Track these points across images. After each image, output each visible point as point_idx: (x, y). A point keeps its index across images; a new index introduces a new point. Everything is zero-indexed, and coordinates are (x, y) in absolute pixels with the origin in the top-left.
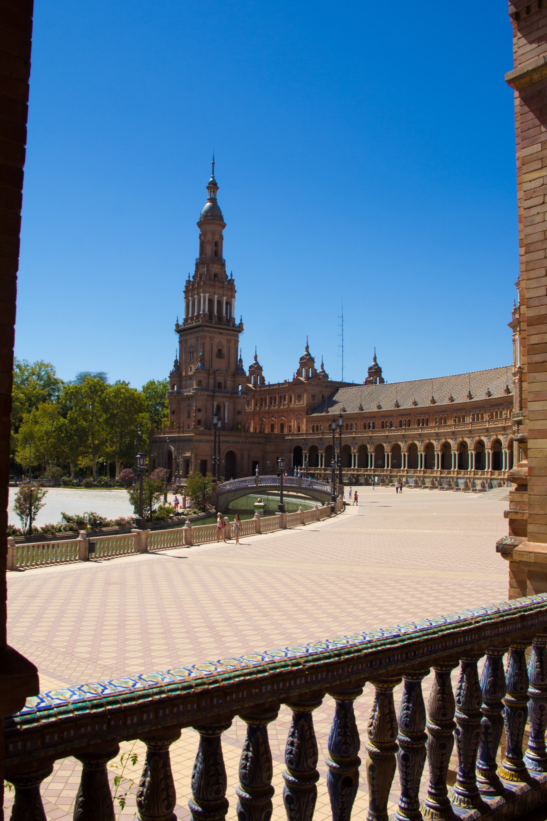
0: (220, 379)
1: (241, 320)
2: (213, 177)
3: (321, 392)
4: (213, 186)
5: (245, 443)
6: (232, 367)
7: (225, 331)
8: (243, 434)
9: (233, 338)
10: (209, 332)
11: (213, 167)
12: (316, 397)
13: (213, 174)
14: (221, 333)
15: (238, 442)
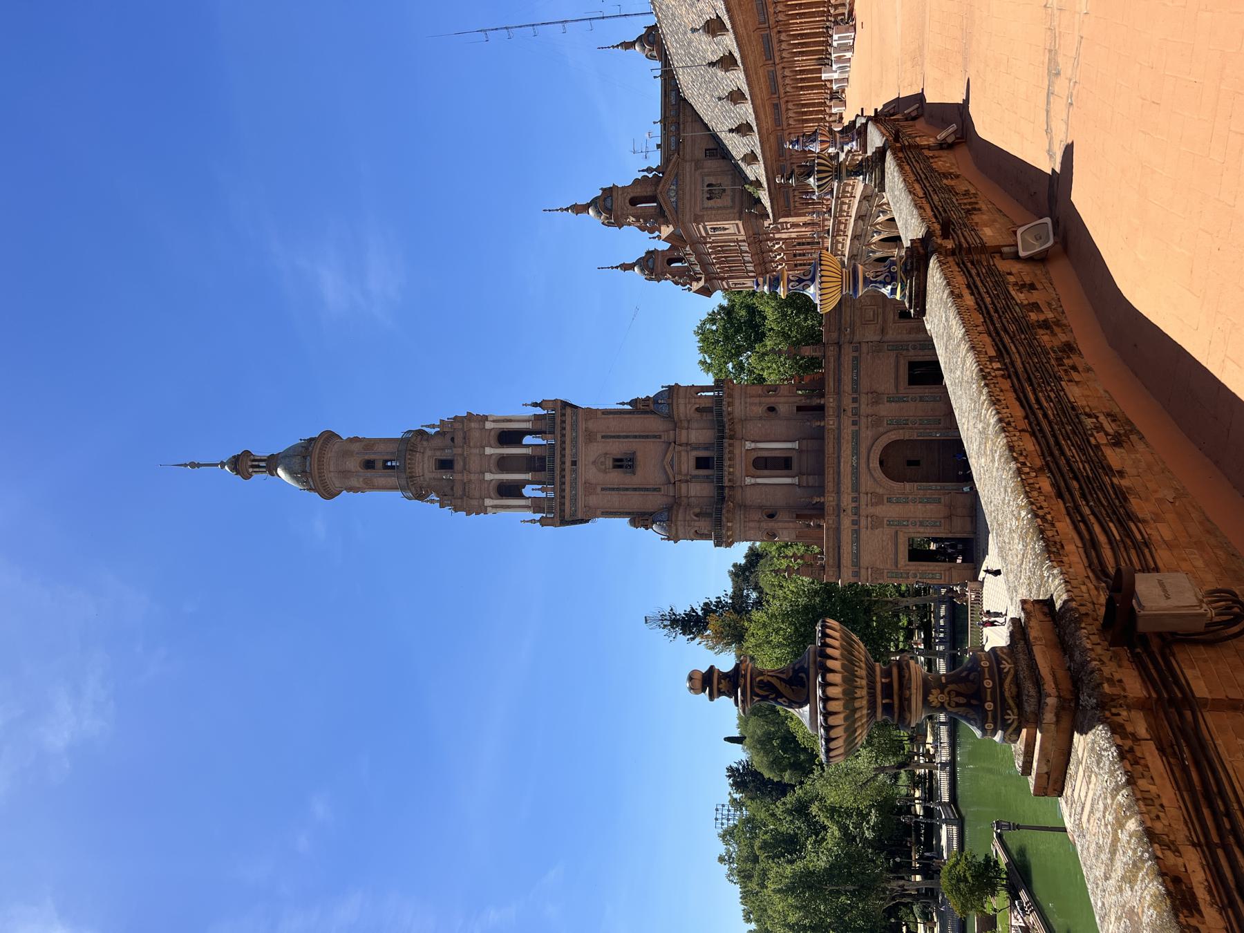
0: (687, 464)
1: (535, 405)
2: (223, 464)
3: (698, 165)
4: (243, 464)
5: (856, 413)
6: (653, 424)
7: (568, 452)
8: (831, 423)
9: (582, 425)
10: (574, 499)
11: (199, 465)
12: (712, 180)
13: (216, 465)
14: (574, 463)
15: (856, 436)
